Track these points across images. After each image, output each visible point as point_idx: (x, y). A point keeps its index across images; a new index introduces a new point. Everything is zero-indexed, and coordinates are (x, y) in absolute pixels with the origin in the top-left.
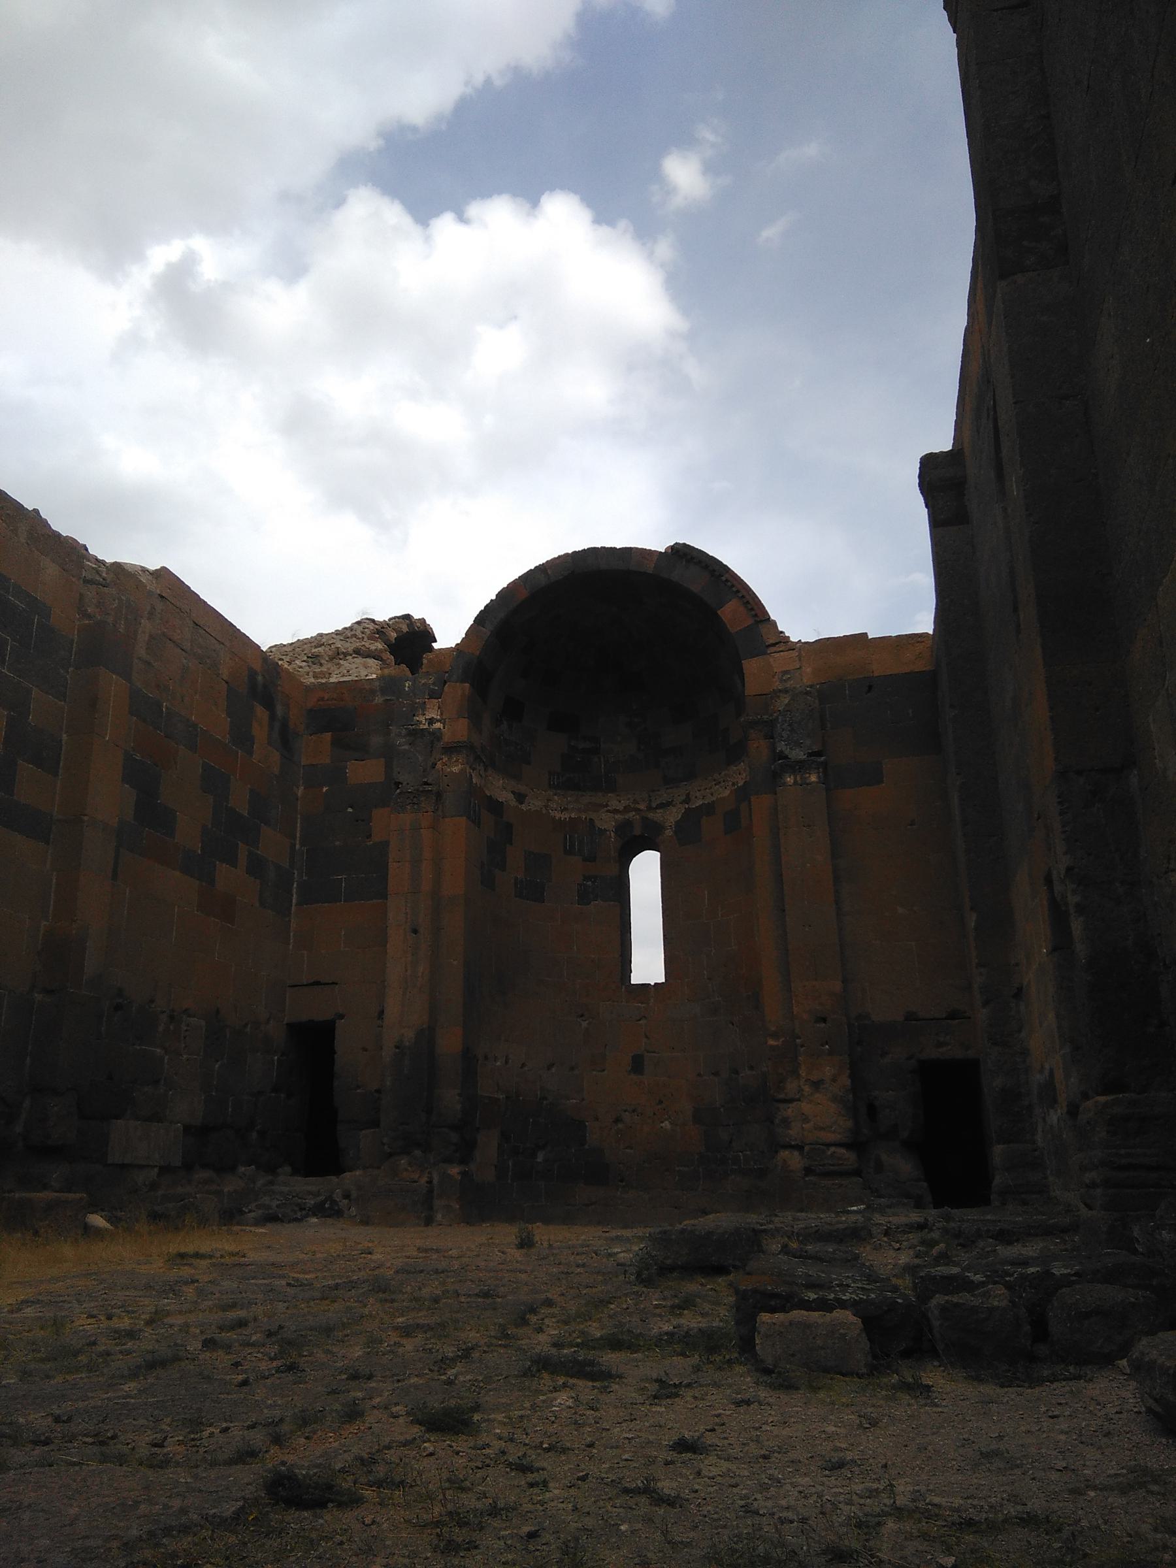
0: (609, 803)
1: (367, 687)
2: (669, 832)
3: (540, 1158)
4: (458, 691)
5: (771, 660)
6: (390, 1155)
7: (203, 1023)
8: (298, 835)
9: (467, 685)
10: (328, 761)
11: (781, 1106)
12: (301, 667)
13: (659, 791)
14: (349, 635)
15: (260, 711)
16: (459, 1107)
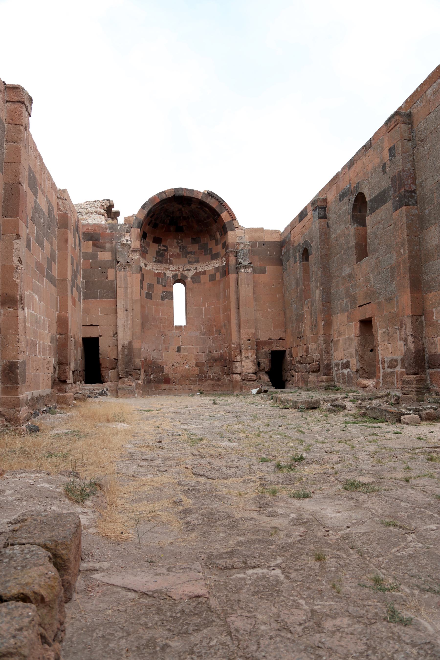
1: (104, 226)
2: (189, 279)
3: (152, 377)
4: (136, 231)
6: (120, 378)
10: (91, 251)
11: (235, 363)
14: (92, 206)
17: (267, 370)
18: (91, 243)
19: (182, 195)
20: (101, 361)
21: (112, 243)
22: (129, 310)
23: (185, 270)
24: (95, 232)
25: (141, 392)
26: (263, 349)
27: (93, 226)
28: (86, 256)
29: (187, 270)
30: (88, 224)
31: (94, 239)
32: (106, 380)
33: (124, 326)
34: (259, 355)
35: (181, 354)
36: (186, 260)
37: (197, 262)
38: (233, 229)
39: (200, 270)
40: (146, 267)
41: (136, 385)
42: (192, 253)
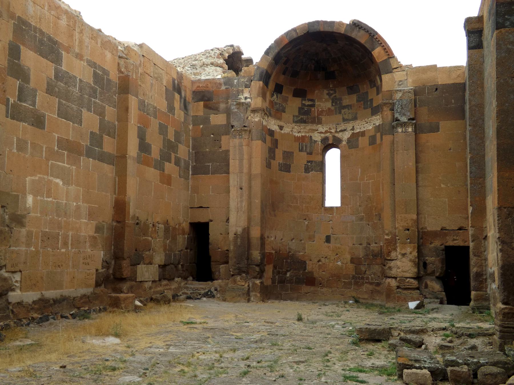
0: (319, 129)
1: (218, 82)
2: (344, 143)
3: (288, 275)
4: (257, 85)
5: (394, 75)
6: (233, 275)
7: (163, 226)
8: (191, 146)
9: (261, 82)
10: (202, 114)
11: (389, 262)
12: (188, 70)
13: (341, 124)
14: (208, 56)
15: (177, 96)
16: (259, 258)
17: (438, 274)
18: (202, 103)
19: (318, 30)
20: (211, 253)
21: (227, 103)
22: (244, 188)
23: (338, 130)
24: (208, 89)
25: (259, 295)
26: (431, 243)
27: (204, 82)
28: (196, 121)
29: (342, 131)
30: (199, 80)
31: (206, 99)
32: (216, 277)
33: (238, 208)
34: (425, 251)
35: (332, 245)
36: (340, 117)
37: (355, 118)
38: (390, 70)
39: (358, 131)
40: (281, 130)
41: (253, 286)
42: (349, 107)
